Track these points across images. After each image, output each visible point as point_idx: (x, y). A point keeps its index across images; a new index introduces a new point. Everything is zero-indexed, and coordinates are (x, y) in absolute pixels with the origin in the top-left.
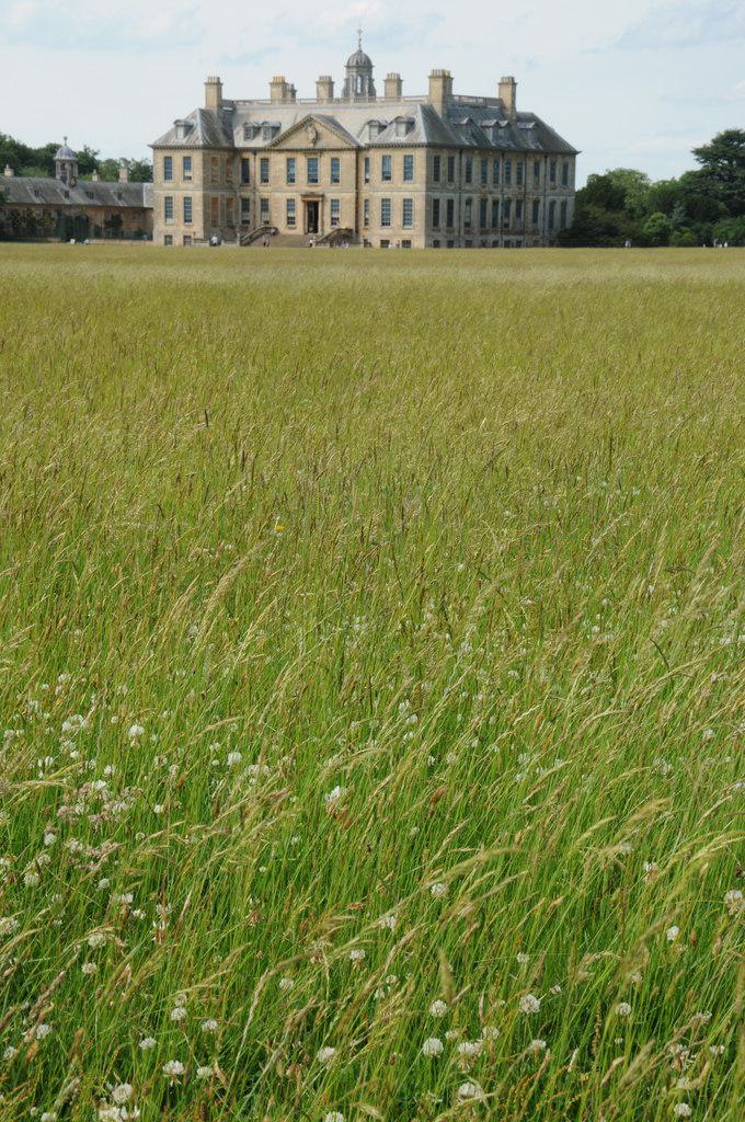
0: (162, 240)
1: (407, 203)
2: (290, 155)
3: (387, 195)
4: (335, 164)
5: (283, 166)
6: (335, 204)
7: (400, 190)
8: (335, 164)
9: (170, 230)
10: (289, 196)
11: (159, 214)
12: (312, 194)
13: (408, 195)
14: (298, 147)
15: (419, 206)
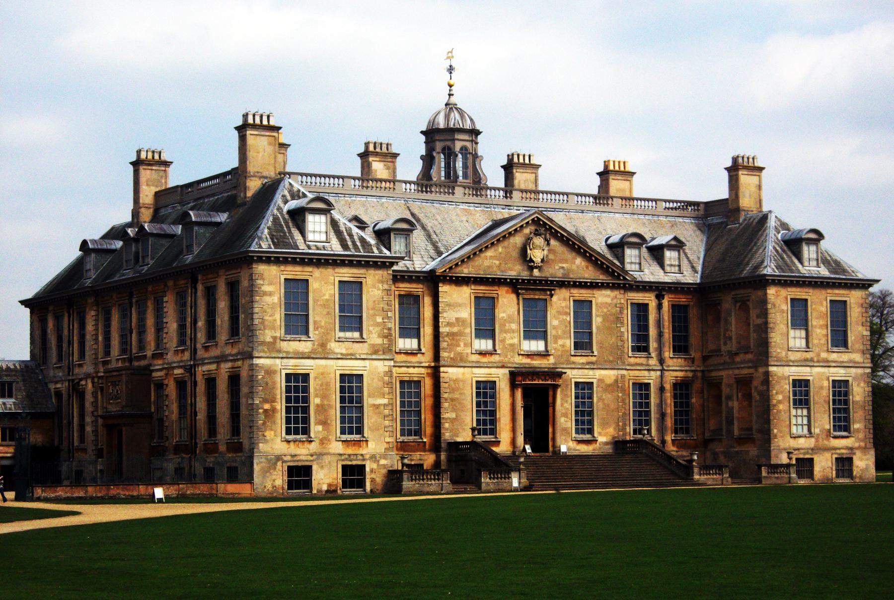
0: (278, 479)
1: (841, 389)
2: (482, 289)
3: (803, 372)
4: (583, 309)
5: (467, 313)
6: (585, 389)
7: (827, 364)
8: (583, 309)
9: (302, 452)
10: (482, 374)
11: (270, 414)
13: (839, 374)
14: (499, 274)
15: (859, 393)
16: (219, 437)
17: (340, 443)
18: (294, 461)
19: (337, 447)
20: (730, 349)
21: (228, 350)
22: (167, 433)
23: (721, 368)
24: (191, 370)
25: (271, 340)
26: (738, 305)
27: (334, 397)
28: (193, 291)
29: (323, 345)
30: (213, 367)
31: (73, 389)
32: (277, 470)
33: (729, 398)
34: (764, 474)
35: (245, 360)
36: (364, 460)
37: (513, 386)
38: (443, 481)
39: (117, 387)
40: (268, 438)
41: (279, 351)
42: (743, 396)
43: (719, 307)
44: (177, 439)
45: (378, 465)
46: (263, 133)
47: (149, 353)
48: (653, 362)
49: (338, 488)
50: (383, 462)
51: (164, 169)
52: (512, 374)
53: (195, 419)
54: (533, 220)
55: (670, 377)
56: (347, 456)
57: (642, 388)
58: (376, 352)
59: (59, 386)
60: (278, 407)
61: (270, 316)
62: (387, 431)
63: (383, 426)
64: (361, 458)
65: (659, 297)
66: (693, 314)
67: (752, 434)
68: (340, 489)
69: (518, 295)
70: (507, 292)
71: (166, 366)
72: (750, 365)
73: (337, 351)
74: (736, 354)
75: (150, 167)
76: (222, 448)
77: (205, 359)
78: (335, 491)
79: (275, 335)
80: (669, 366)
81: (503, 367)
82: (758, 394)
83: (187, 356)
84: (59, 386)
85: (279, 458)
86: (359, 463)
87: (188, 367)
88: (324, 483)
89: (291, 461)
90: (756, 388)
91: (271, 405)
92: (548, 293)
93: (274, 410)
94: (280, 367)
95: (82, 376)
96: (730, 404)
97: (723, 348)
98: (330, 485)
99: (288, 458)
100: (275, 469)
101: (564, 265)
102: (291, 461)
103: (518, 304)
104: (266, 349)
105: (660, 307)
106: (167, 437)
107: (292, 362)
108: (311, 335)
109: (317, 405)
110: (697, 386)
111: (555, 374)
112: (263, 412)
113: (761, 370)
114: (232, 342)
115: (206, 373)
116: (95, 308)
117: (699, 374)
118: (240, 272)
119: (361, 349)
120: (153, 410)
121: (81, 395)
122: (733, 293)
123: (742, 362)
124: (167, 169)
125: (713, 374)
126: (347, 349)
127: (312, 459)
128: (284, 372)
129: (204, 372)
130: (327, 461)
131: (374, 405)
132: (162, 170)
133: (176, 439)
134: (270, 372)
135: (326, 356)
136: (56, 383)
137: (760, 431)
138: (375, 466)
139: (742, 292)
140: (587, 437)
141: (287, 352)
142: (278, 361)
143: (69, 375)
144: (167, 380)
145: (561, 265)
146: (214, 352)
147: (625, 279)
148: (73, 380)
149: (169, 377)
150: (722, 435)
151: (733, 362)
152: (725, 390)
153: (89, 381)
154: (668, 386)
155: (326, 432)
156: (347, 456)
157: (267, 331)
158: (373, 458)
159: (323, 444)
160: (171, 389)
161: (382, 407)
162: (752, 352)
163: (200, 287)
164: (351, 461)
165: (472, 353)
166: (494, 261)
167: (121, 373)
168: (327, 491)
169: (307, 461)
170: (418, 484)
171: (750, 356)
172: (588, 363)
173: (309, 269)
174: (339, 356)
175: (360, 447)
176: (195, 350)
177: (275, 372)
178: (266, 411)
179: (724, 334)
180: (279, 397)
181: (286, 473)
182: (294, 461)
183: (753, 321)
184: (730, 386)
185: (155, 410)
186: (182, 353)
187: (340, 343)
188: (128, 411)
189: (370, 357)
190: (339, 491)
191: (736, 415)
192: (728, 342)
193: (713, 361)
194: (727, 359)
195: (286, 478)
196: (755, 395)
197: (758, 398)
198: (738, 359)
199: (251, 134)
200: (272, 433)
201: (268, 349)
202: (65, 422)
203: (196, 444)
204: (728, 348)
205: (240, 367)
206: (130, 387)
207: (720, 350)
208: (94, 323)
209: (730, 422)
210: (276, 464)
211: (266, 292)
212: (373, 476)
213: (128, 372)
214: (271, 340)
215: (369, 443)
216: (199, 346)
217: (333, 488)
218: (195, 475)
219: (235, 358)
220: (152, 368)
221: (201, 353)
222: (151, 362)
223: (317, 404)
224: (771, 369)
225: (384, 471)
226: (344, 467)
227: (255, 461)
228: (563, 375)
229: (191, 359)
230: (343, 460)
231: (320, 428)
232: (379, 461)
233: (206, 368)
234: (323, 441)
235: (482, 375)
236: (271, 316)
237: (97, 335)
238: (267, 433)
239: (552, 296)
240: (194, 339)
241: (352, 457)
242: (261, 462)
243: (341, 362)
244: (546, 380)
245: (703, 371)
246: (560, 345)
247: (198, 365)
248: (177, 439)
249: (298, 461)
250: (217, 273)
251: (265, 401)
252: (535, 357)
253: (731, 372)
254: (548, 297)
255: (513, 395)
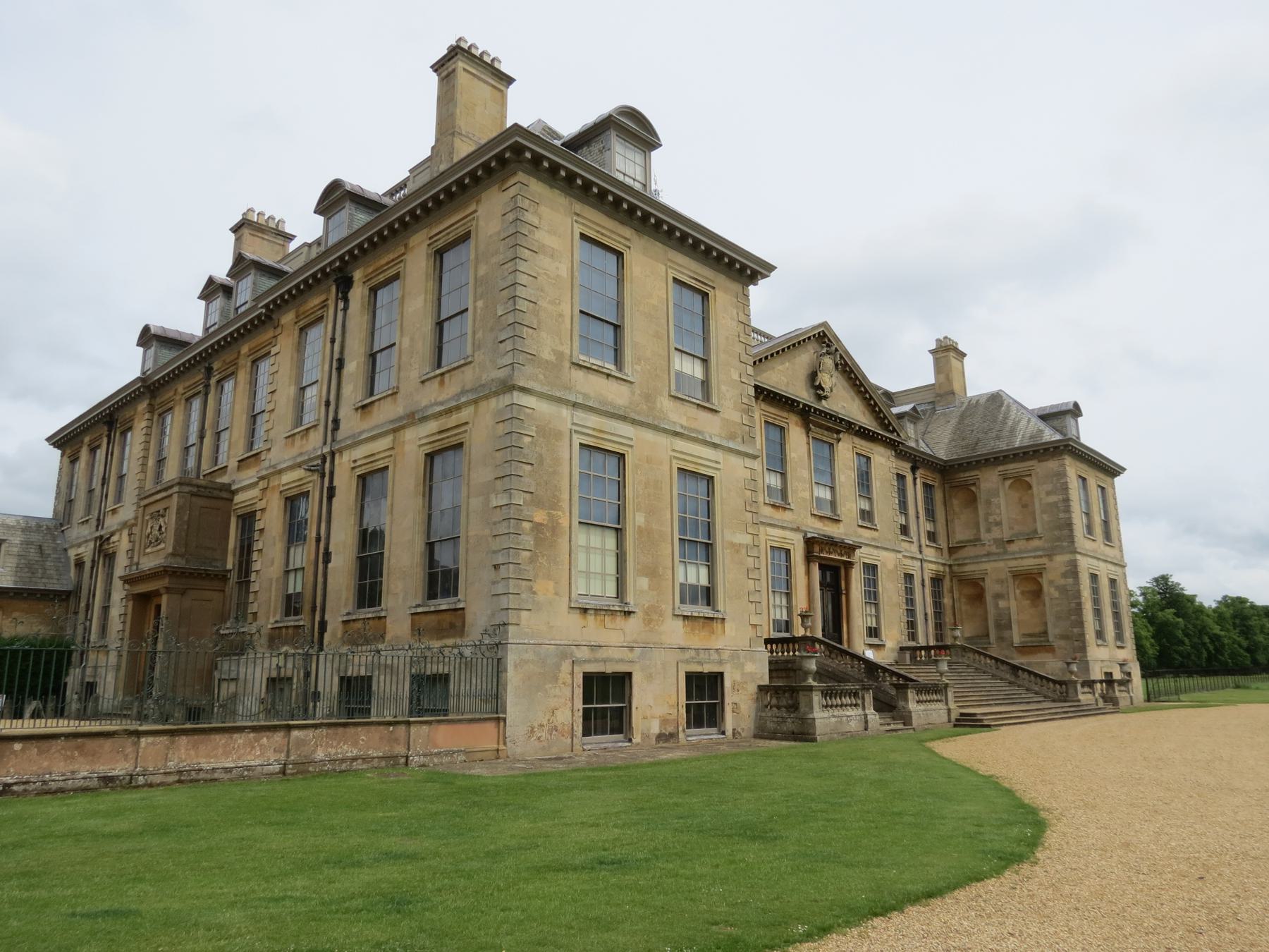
12: (831, 543)
16: (388, 601)
17: (680, 623)
18: (596, 661)
19: (675, 632)
20: (999, 537)
21: (431, 396)
22: (256, 605)
23: (984, 560)
24: (322, 467)
25: (553, 358)
26: (1008, 483)
27: (669, 516)
28: (341, 305)
29: (649, 398)
30: (385, 442)
31: (99, 552)
32: (560, 681)
33: (998, 596)
34: (1117, 694)
35: (483, 405)
36: (721, 662)
37: (809, 558)
38: (864, 708)
39: (161, 520)
40: (540, 597)
41: (569, 388)
42: (1023, 593)
43: (973, 488)
44: (278, 618)
45: (743, 674)
46: (483, 76)
47: (233, 464)
48: (914, 548)
49: (680, 729)
50: (749, 667)
51: (282, 243)
52: (810, 542)
53: (326, 568)
54: (819, 333)
55: (930, 570)
56: (693, 653)
57: (909, 577)
58: (732, 437)
59: (81, 550)
60: (564, 522)
61: (550, 302)
62: (752, 602)
63: (746, 591)
64: (715, 656)
65: (914, 469)
66: (938, 496)
67: (1048, 641)
68: (684, 731)
69: (808, 431)
70: (797, 424)
71: (264, 473)
72: (1040, 553)
73: (674, 417)
74: (1010, 542)
75: (260, 235)
76: (398, 626)
77: (361, 433)
78: (672, 736)
79: (561, 348)
80: (926, 556)
81: (797, 530)
82: (1056, 590)
83: (316, 438)
84: (81, 550)
85: (564, 652)
86: (716, 669)
87: (315, 463)
88: (653, 717)
89: (589, 661)
90: (1051, 582)
91: (549, 514)
92: (835, 436)
93: (554, 528)
94: (569, 426)
95: (115, 528)
96: (1002, 604)
97: (985, 536)
98: (664, 721)
99: (583, 653)
100: (556, 679)
101: (845, 405)
102: (589, 661)
103: (808, 444)
104: (541, 377)
105: (915, 479)
106: (255, 614)
107: (593, 421)
108: (628, 368)
109: (640, 531)
110: (947, 583)
111: (851, 549)
112: (532, 529)
113: (1061, 559)
114: (442, 374)
115: (359, 463)
116: (147, 416)
117: (947, 569)
118: (475, 211)
119: (710, 426)
120: (229, 566)
121: (110, 558)
122: (1001, 468)
123: (1021, 552)
124: (285, 244)
125: (967, 568)
126: (688, 418)
127: (630, 656)
128: (577, 440)
129: (355, 461)
130: (659, 662)
131: (733, 545)
132: (280, 244)
133: (274, 616)
134: (548, 433)
135: (656, 423)
136: (79, 545)
137: (1065, 637)
138: (738, 677)
139: (1013, 467)
140: (875, 641)
141: (586, 396)
142: (565, 412)
143: (97, 530)
144: (264, 501)
145: (843, 404)
146: (386, 413)
147: (898, 435)
148: (101, 537)
149: (268, 492)
150: (990, 643)
151: (1005, 552)
152: (991, 587)
153: (125, 533)
154: (927, 582)
155: (655, 593)
156: (693, 653)
157: (544, 335)
158: (735, 655)
159: (650, 621)
160: (272, 521)
161: (744, 551)
162: (1041, 538)
163: (358, 293)
164: (700, 663)
165: (765, 503)
166: (782, 378)
167: (170, 492)
168: (660, 737)
169: (622, 661)
170: (834, 717)
171: (1036, 543)
172: (874, 539)
173: (627, 232)
174: (679, 430)
175: (713, 633)
176: (336, 422)
177: (558, 435)
178: (537, 527)
179: (986, 520)
180: (566, 496)
181: (579, 692)
182: (596, 661)
183: (1041, 499)
184: (1001, 581)
185: (234, 566)
186: (302, 438)
187: (678, 404)
188: (179, 563)
189: (724, 443)
190: (681, 735)
191: (1014, 617)
192: (995, 529)
193: (969, 552)
194: (994, 549)
195: (579, 705)
196: (1050, 591)
197: (1056, 594)
198: (1013, 548)
199: (464, 69)
200: (551, 585)
201: (544, 375)
202: (83, 605)
203: (323, 625)
204: (996, 533)
205: (467, 423)
206: (186, 518)
207: (979, 539)
208: (143, 438)
209: (1004, 624)
210: (558, 667)
211: (543, 245)
212: (736, 699)
213: (187, 489)
214: (553, 358)
215: (727, 625)
216: (346, 412)
217: (670, 729)
218: (316, 695)
219: (453, 404)
220: (234, 487)
221: (350, 423)
222: (234, 478)
223: (639, 527)
224: (1078, 557)
225: (752, 688)
226: (690, 677)
227: (511, 659)
228: (857, 551)
229: (325, 443)
230: (687, 662)
231: (644, 582)
232: (743, 665)
233: (359, 453)
234: (652, 615)
235: (776, 539)
236: (552, 303)
237: (145, 458)
238: (539, 586)
239: (839, 440)
240: (331, 404)
241: (702, 655)
242: (527, 662)
243: (680, 444)
244: (830, 553)
245: (950, 566)
246: (849, 510)
247: (341, 451)
248: (278, 618)
249: (605, 661)
250: (406, 246)
251: (538, 503)
252: (826, 522)
253: (1001, 564)
254: (834, 442)
255: (808, 572)
